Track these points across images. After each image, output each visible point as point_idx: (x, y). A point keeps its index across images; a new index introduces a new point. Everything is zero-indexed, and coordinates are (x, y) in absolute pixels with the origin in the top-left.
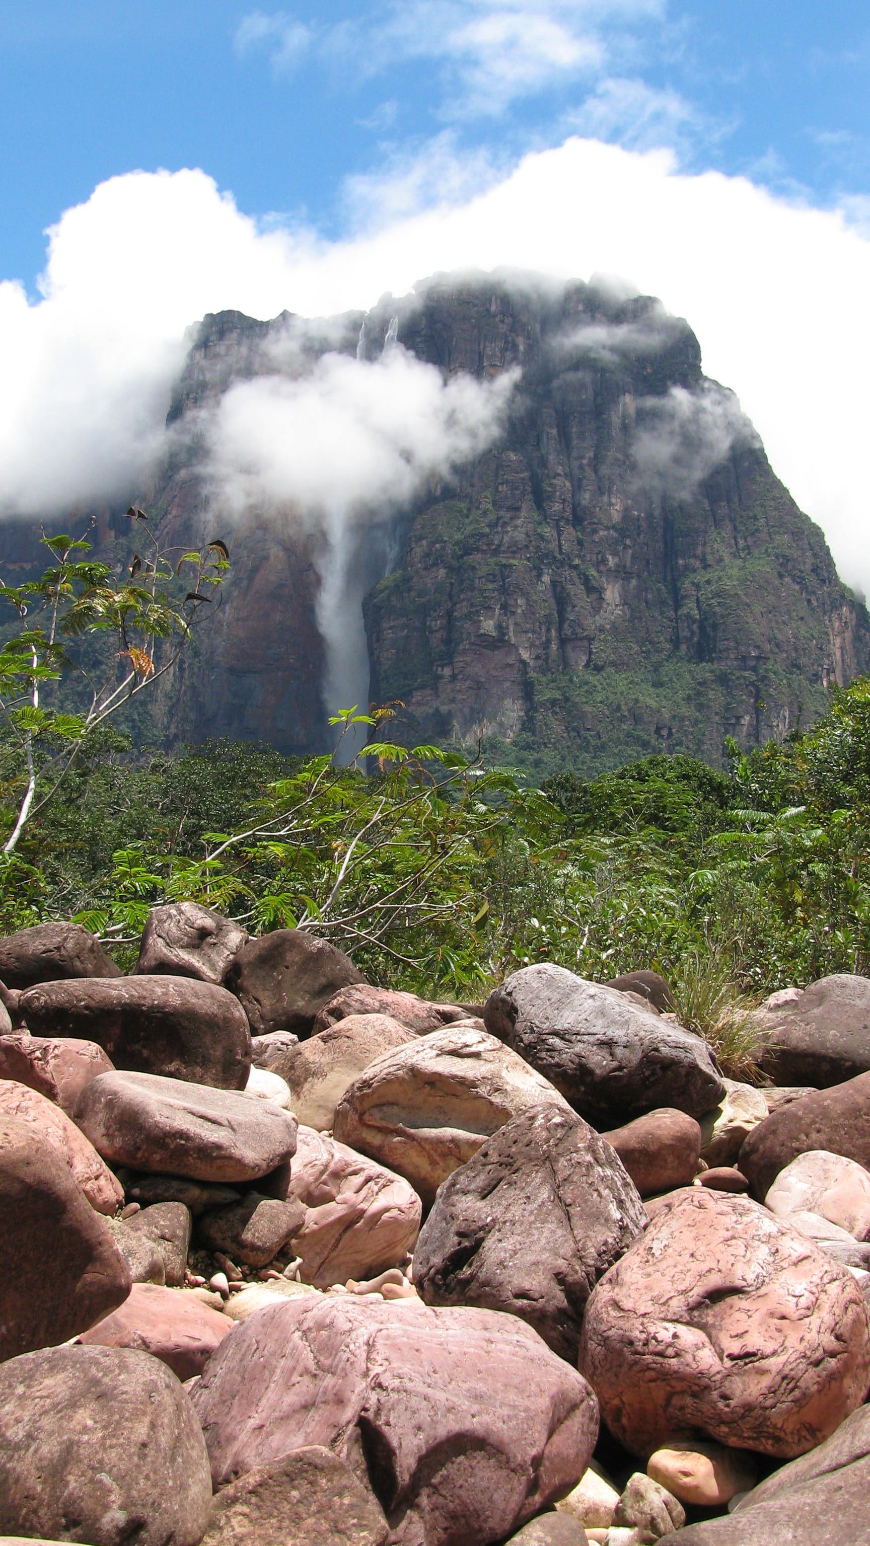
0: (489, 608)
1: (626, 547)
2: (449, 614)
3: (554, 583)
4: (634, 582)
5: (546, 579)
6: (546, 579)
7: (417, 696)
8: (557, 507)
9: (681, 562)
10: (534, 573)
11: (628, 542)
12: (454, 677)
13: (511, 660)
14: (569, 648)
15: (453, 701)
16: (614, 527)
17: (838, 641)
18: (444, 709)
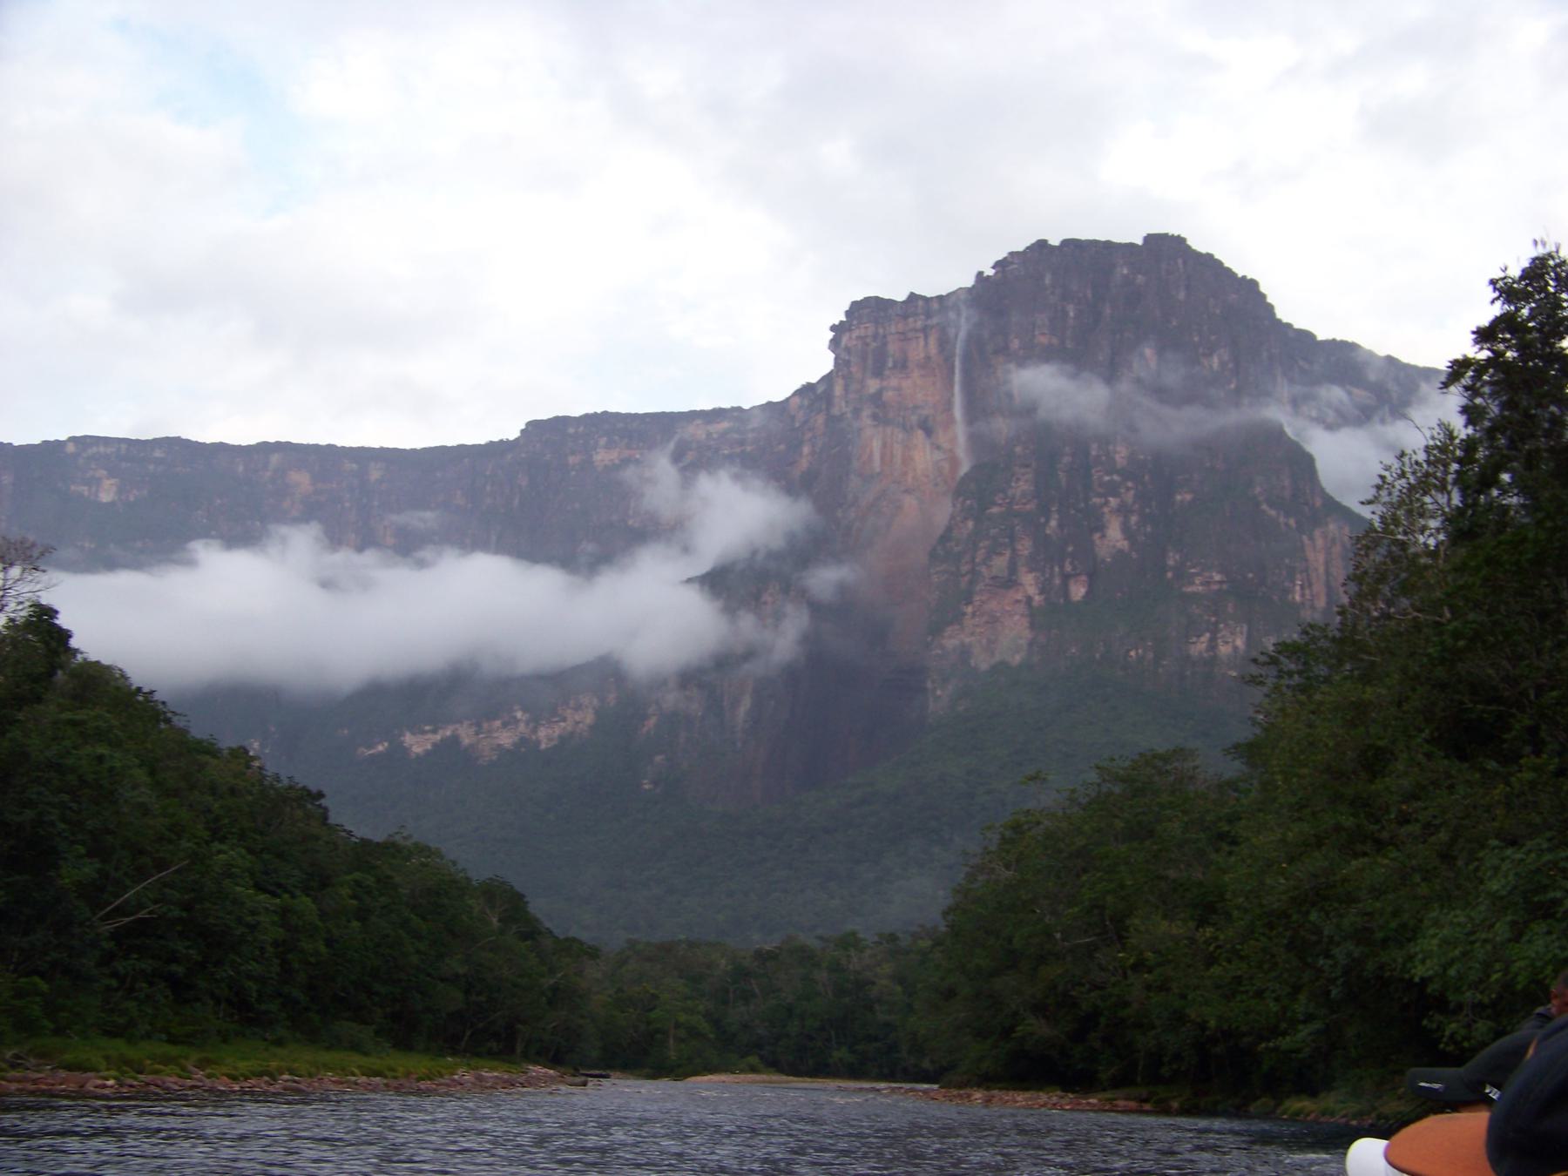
0: (1001, 554)
1: (1128, 489)
2: (973, 560)
3: (1061, 526)
4: (1134, 519)
5: (1053, 523)
6: (1053, 523)
7: (949, 630)
8: (1066, 459)
9: (1179, 498)
10: (1043, 520)
11: (1130, 484)
12: (974, 615)
13: (1019, 596)
14: (1072, 582)
15: (972, 634)
16: (1117, 472)
17: (1321, 558)
18: (967, 640)
